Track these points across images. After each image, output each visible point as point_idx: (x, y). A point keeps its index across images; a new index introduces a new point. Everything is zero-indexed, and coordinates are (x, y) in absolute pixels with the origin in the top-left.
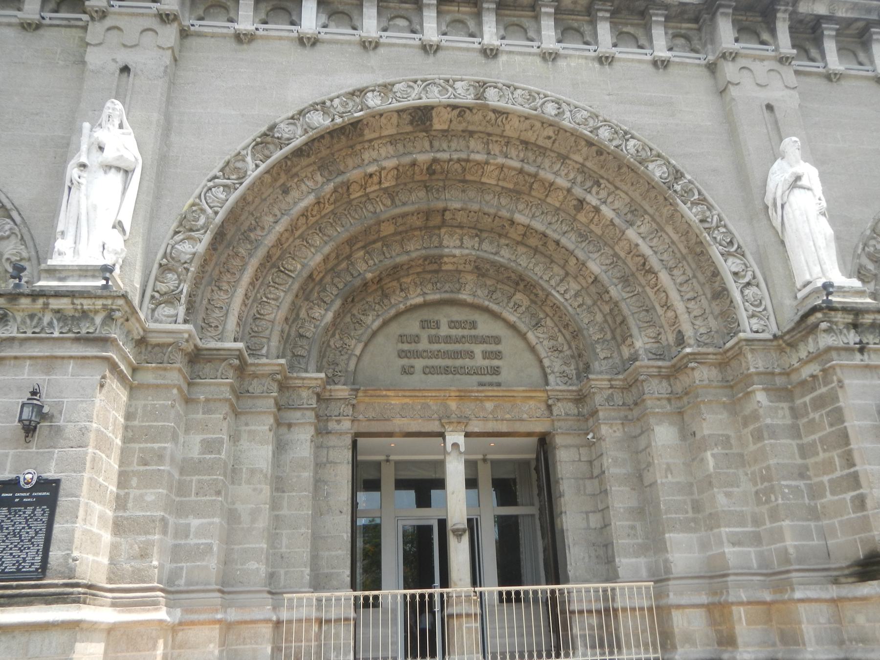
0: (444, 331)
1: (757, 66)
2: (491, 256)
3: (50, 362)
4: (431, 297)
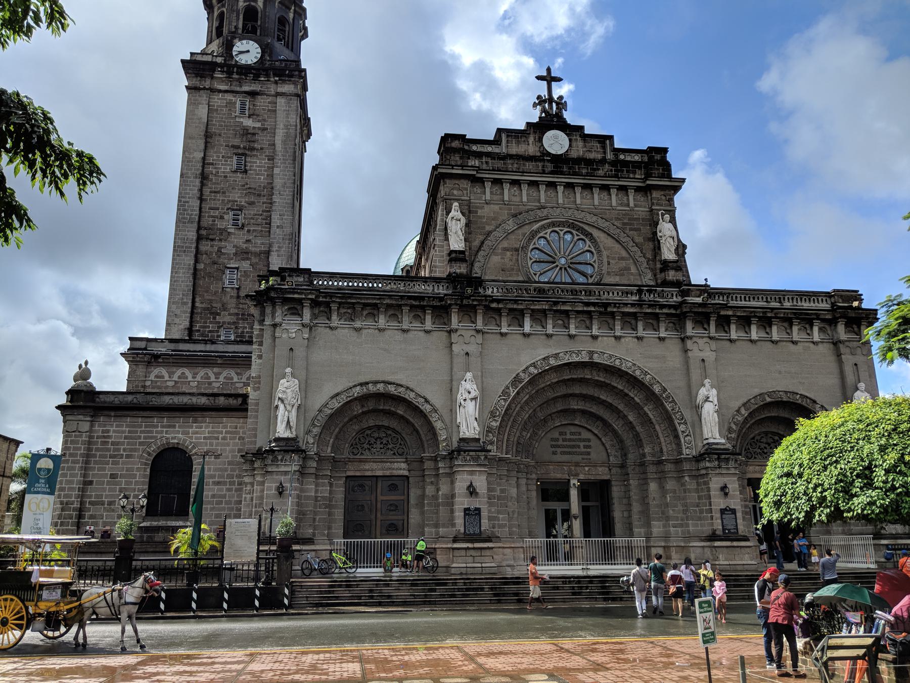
0: (568, 436)
1: (700, 341)
2: (589, 409)
3: (472, 473)
4: (563, 423)
